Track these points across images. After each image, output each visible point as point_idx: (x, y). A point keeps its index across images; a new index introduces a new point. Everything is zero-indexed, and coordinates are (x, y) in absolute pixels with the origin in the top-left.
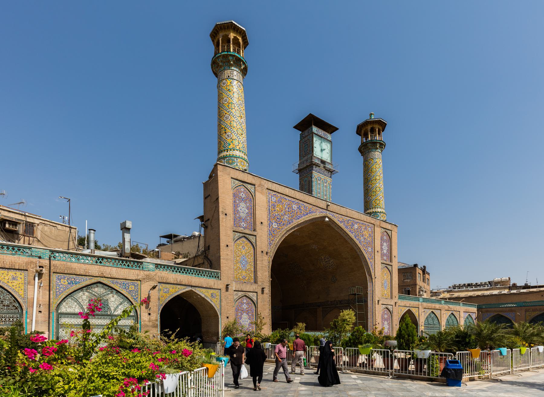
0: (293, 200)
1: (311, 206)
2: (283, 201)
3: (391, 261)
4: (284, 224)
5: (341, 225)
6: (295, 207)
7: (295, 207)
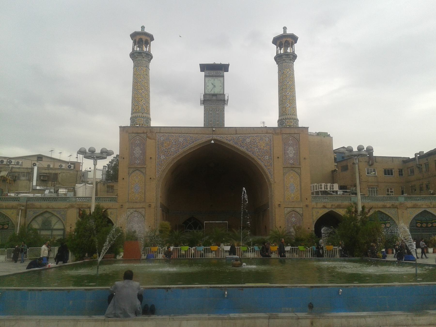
0: (179, 135)
1: (197, 135)
3: (300, 164)
5: (231, 143)
6: (181, 140)
7: (181, 140)
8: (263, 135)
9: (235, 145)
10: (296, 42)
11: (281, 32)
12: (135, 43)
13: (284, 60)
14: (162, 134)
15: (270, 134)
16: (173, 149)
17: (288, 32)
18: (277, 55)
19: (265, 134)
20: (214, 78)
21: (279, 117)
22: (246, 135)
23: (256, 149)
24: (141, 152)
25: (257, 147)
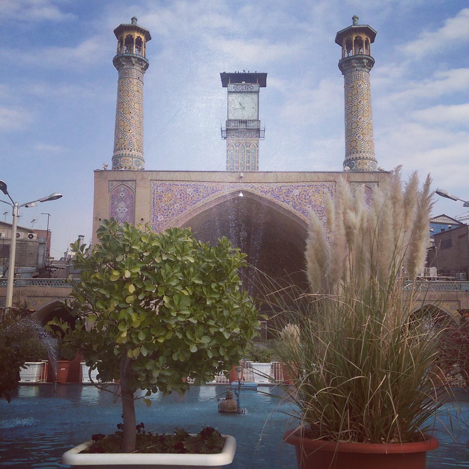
1: (214, 184)
2: (173, 188)
4: (173, 214)
5: (268, 196)
7: (189, 191)
8: (319, 184)
9: (275, 200)
10: (372, 41)
11: (349, 24)
12: (121, 41)
13: (354, 67)
14: (160, 182)
15: (331, 183)
16: (177, 206)
17: (362, 22)
18: (343, 59)
19: (324, 183)
20: (243, 95)
21: (346, 156)
22: (293, 184)
23: (308, 205)
24: (127, 210)
25: (310, 202)
